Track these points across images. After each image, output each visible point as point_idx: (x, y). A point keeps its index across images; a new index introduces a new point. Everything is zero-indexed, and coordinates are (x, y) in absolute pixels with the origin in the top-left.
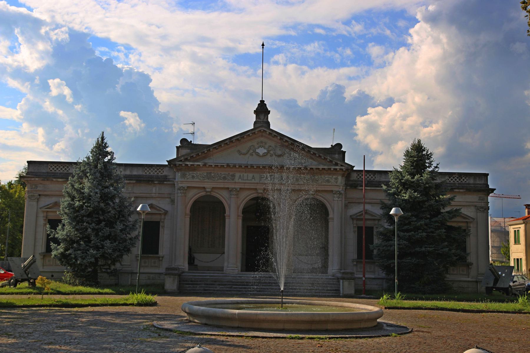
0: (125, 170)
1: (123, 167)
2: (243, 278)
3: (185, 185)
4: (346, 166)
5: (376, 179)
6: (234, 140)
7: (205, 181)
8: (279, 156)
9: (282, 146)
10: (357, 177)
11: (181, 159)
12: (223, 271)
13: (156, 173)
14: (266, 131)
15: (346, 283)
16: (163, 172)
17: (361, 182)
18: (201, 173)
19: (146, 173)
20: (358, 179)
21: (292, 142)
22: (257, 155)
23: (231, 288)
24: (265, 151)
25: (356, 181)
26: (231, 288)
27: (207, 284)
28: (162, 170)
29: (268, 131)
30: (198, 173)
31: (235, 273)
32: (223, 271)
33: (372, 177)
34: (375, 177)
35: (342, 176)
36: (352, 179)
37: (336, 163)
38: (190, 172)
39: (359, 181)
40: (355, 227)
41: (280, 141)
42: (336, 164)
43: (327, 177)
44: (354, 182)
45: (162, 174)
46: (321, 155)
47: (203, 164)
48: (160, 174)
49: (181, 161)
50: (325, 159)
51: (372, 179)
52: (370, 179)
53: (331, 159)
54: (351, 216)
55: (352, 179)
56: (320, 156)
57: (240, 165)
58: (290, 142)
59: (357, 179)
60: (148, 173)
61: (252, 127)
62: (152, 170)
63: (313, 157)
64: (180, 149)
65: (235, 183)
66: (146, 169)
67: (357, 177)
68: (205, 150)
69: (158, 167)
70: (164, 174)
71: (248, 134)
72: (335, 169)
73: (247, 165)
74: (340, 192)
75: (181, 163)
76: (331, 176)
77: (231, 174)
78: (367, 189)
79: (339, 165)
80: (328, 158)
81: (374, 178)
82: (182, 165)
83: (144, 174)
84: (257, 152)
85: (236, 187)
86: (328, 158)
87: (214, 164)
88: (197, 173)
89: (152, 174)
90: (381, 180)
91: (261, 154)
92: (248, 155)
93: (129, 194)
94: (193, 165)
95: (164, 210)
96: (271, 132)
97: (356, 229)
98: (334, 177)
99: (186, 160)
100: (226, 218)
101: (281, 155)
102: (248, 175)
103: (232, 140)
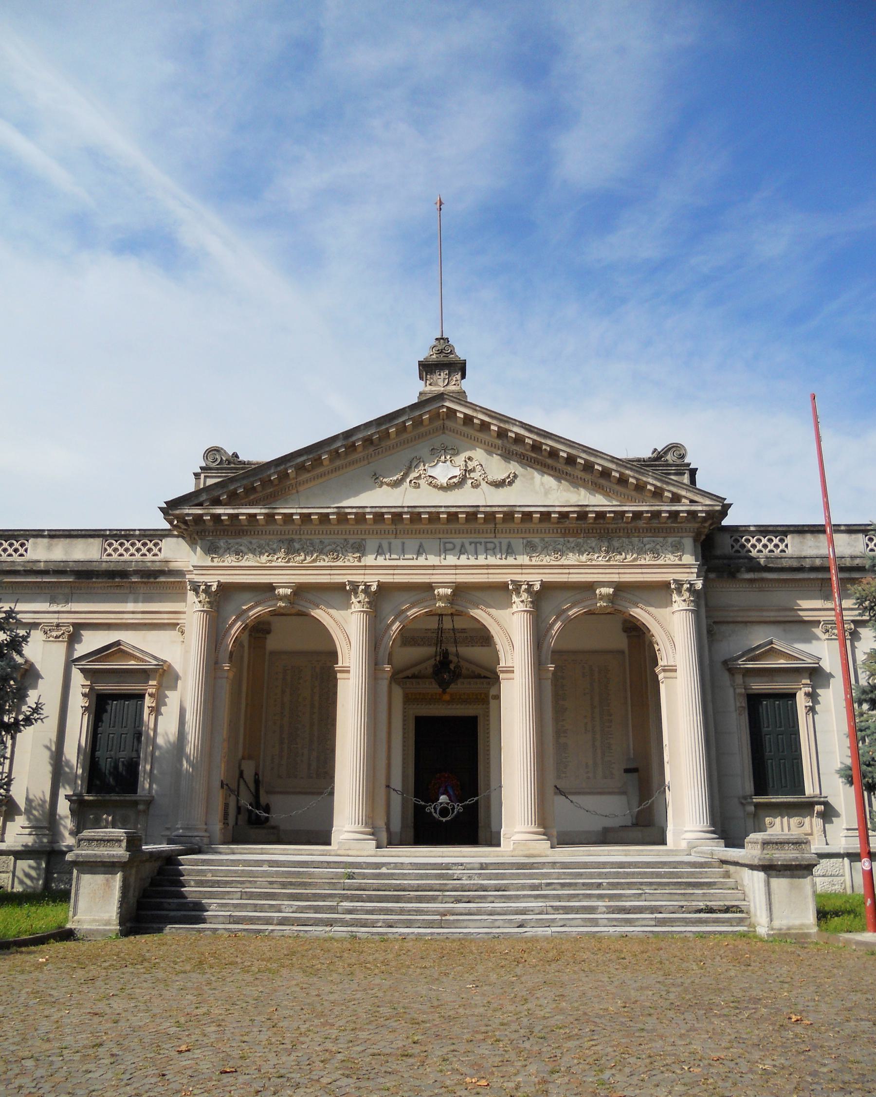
0: (49, 548)
1: (46, 540)
2: (384, 870)
3: (213, 579)
4: (708, 502)
5: (790, 552)
6: (358, 440)
7: (274, 564)
8: (499, 484)
9: (507, 456)
10: (733, 547)
11: (202, 499)
12: (329, 844)
13: (138, 556)
14: (455, 411)
15: (780, 884)
16: (160, 550)
17: (746, 561)
18: (262, 542)
19: (110, 555)
20: (738, 551)
21: (535, 437)
22: (430, 484)
23: (332, 910)
24: (457, 472)
25: (730, 558)
26: (332, 910)
27: (251, 896)
28: (156, 545)
29: (462, 411)
30: (254, 541)
31: (365, 853)
32: (329, 844)
33: (776, 546)
34: (787, 546)
35: (695, 540)
36: (718, 552)
37: (673, 494)
38: (230, 541)
39: (739, 558)
40: (740, 694)
41: (499, 442)
42: (676, 499)
43: (649, 543)
44: (725, 561)
45: (155, 558)
46: (628, 472)
47: (263, 511)
48: (150, 557)
49: (200, 504)
50: (640, 488)
51: (777, 552)
52: (771, 551)
53: (659, 484)
54: (725, 663)
55: (718, 552)
56: (623, 481)
57: (377, 510)
58: (530, 438)
59: (732, 552)
60: (115, 556)
61: (416, 401)
62: (127, 545)
63: (602, 481)
64: (202, 476)
65: (365, 567)
66: (110, 545)
67: (733, 547)
68: (272, 471)
69: (145, 536)
70: (161, 556)
71: (401, 420)
72: (674, 515)
73: (399, 510)
74: (691, 585)
75: (200, 512)
76: (661, 539)
77: (351, 541)
78: (771, 580)
79: (684, 500)
80: (651, 480)
81: (782, 547)
82: (201, 515)
83: (105, 558)
84: (430, 476)
85: (367, 579)
86: (651, 480)
87: (299, 511)
88: (251, 543)
89: (126, 557)
90: (804, 554)
91: (443, 480)
92: (406, 484)
93: (56, 615)
94: (237, 515)
95: (155, 658)
96: (469, 412)
97: (744, 704)
98: (670, 540)
99: (217, 502)
100: (339, 675)
101: (504, 480)
102: (403, 543)
103: (354, 438)
